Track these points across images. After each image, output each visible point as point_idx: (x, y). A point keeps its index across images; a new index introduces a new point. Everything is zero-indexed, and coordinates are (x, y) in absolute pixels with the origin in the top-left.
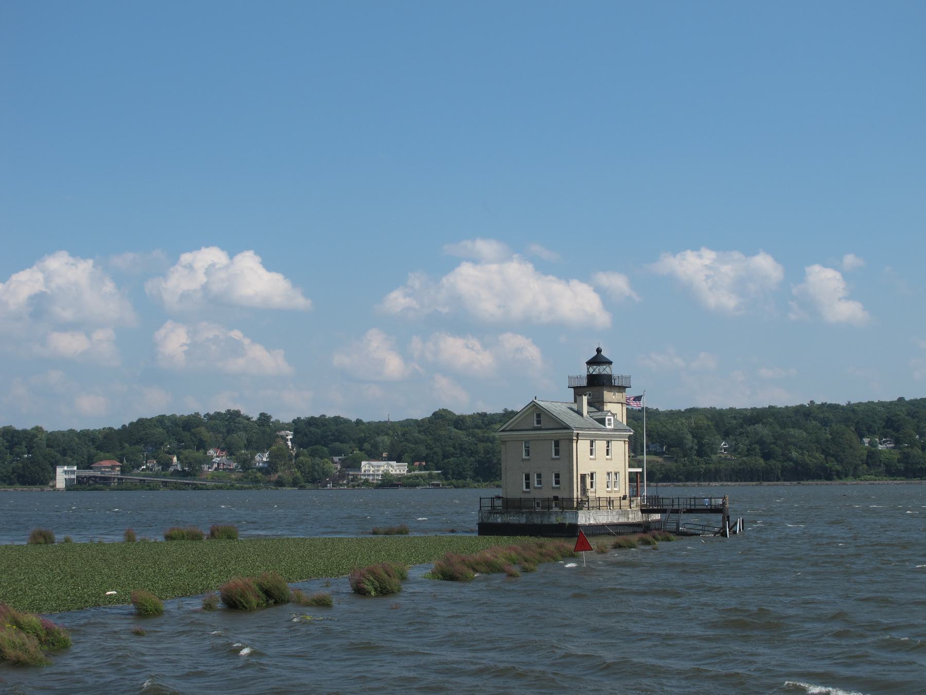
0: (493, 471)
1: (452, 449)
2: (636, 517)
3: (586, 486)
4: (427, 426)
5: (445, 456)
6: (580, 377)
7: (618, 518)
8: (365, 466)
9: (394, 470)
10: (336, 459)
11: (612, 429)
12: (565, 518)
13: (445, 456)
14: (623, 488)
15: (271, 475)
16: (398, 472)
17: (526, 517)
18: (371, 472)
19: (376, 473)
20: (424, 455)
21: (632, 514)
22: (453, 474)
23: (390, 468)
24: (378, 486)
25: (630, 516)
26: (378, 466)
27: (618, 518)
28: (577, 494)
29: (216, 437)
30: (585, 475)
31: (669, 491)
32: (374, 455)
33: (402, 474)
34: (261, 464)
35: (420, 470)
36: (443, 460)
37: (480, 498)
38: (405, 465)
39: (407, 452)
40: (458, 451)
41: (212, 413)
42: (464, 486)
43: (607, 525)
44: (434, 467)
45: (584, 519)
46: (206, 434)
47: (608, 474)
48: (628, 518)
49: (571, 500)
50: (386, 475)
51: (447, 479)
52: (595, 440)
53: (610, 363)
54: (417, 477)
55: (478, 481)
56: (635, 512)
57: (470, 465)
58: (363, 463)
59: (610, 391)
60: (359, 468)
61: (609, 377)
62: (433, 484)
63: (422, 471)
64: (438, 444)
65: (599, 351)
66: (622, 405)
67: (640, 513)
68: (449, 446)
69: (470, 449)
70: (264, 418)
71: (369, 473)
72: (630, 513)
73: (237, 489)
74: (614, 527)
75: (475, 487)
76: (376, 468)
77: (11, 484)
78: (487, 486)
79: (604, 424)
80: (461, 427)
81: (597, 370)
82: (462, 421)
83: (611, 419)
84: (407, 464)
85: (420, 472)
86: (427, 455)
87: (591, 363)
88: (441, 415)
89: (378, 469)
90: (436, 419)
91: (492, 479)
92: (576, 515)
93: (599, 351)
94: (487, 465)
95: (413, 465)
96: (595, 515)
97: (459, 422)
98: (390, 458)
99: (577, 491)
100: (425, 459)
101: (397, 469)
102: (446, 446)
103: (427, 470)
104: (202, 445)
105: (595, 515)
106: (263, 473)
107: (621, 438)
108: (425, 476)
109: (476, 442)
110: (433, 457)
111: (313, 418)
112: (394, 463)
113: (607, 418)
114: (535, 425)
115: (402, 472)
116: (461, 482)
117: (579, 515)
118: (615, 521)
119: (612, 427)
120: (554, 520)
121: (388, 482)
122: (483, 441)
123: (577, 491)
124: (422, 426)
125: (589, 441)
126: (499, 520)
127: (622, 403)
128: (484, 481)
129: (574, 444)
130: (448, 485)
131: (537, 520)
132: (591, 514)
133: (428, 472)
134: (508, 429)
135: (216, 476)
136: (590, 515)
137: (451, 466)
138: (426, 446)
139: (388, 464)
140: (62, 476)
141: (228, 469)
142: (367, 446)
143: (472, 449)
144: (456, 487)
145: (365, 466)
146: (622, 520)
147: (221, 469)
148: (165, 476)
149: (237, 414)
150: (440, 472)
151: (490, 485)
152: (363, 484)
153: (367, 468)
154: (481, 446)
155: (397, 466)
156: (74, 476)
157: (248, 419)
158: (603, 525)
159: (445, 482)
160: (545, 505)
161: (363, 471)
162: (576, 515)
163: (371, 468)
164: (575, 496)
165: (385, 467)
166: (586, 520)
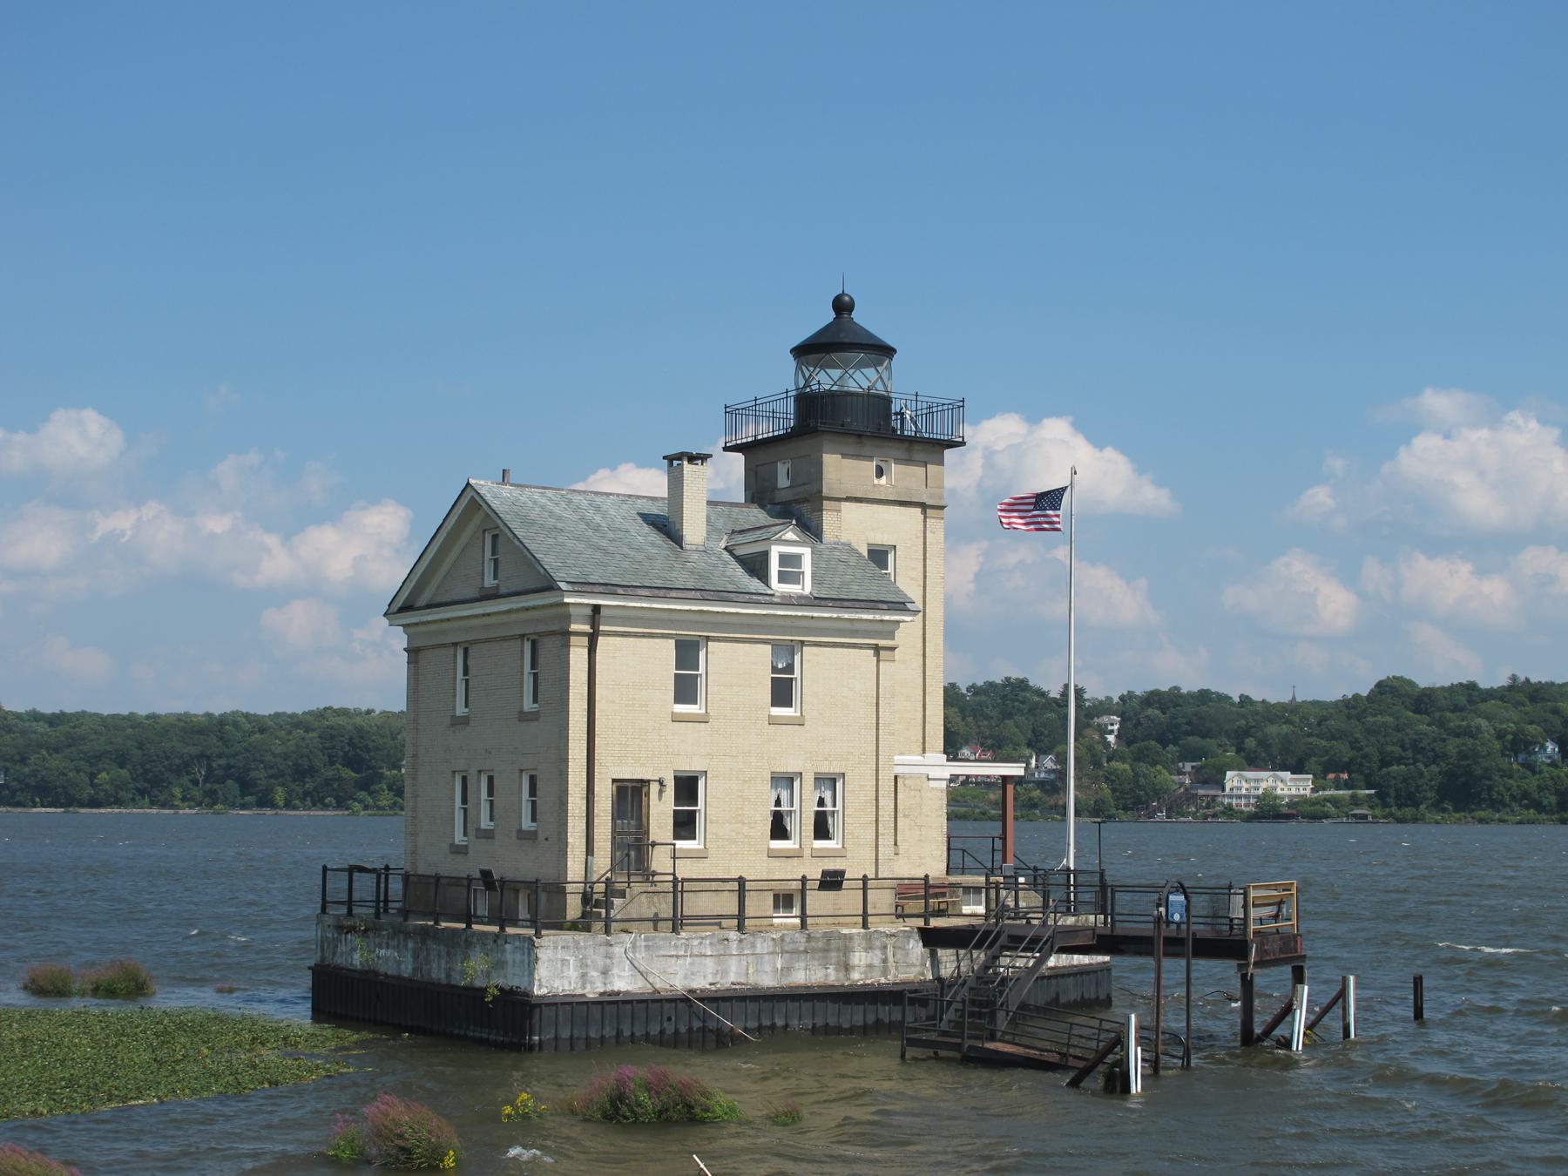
0: (1473, 791)
1: (1397, 750)
3: (647, 832)
4: (1363, 707)
6: (754, 409)
7: (787, 970)
8: (1232, 779)
9: (1286, 789)
11: (801, 597)
12: (500, 965)
13: (1385, 763)
15: (1059, 794)
16: (1294, 791)
17: (414, 950)
18: (1244, 792)
19: (1253, 792)
20: (1346, 759)
21: (869, 948)
22: (1398, 797)
23: (1279, 783)
24: (1251, 818)
25: (859, 958)
26: (1257, 780)
27: (787, 970)
29: (979, 727)
30: (645, 783)
32: (1253, 762)
33: (1302, 796)
34: (1043, 775)
35: (1338, 788)
36: (1380, 769)
37: (325, 869)
38: (1309, 779)
39: (1315, 755)
40: (1410, 754)
41: (980, 683)
42: (1415, 820)
43: (701, 1000)
44: (1362, 783)
45: (573, 973)
47: (785, 780)
48: (847, 968)
49: (558, 889)
51: (1385, 805)
52: (708, 639)
53: (885, 351)
55: (1444, 810)
56: (890, 942)
57: (1431, 780)
58: (1229, 774)
59: (858, 457)
61: (880, 405)
62: (1355, 816)
63: (1341, 789)
64: (1373, 739)
65: (842, 306)
66: (924, 513)
67: (916, 948)
68: (1394, 744)
69: (1433, 750)
71: (1239, 793)
72: (857, 943)
74: (752, 1007)
75: (1437, 822)
76: (1252, 784)
78: (1460, 819)
79: (763, 576)
80: (1426, 708)
81: (825, 379)
82: (1430, 697)
83: (785, 559)
84: (1311, 776)
85: (1336, 792)
86: (1352, 760)
87: (809, 351)
88: (1391, 687)
89: (1256, 785)
90: (1381, 694)
91: (1473, 807)
92: (529, 954)
93: (842, 306)
94: (1463, 779)
95: (1324, 778)
96: (640, 955)
97: (1424, 701)
99: (590, 850)
100: (1346, 767)
102: (1387, 744)
103: (1349, 789)
105: (640, 955)
106: (1046, 792)
107: (855, 634)
108: (1344, 800)
109: (1445, 736)
110: (1361, 765)
112: (1287, 775)
113: (775, 552)
114: (489, 581)
115: (1302, 792)
117: (541, 954)
118: (767, 979)
119: (806, 587)
121: (1268, 811)
122: (1457, 735)
123: (590, 850)
124: (1354, 707)
125: (672, 643)
126: (357, 960)
127: (923, 506)
128: (1456, 810)
129: (578, 656)
130: (1385, 817)
132: (618, 950)
133: (1350, 792)
134: (422, 602)
135: (961, 795)
136: (609, 956)
137: (1393, 782)
138: (1350, 742)
139: (1275, 776)
141: (984, 783)
142: (1250, 743)
143: (1437, 749)
144: (1400, 821)
145: (1232, 779)
146: (808, 974)
147: (971, 782)
149: (1022, 685)
150: (1373, 792)
151: (1466, 817)
152: (1223, 813)
153: (1235, 784)
155: (1291, 780)
157: (1042, 694)
158: (685, 1002)
159: (1378, 812)
161: (1227, 789)
162: (529, 954)
163: (1242, 784)
164: (575, 869)
165: (1271, 783)
166: (583, 975)
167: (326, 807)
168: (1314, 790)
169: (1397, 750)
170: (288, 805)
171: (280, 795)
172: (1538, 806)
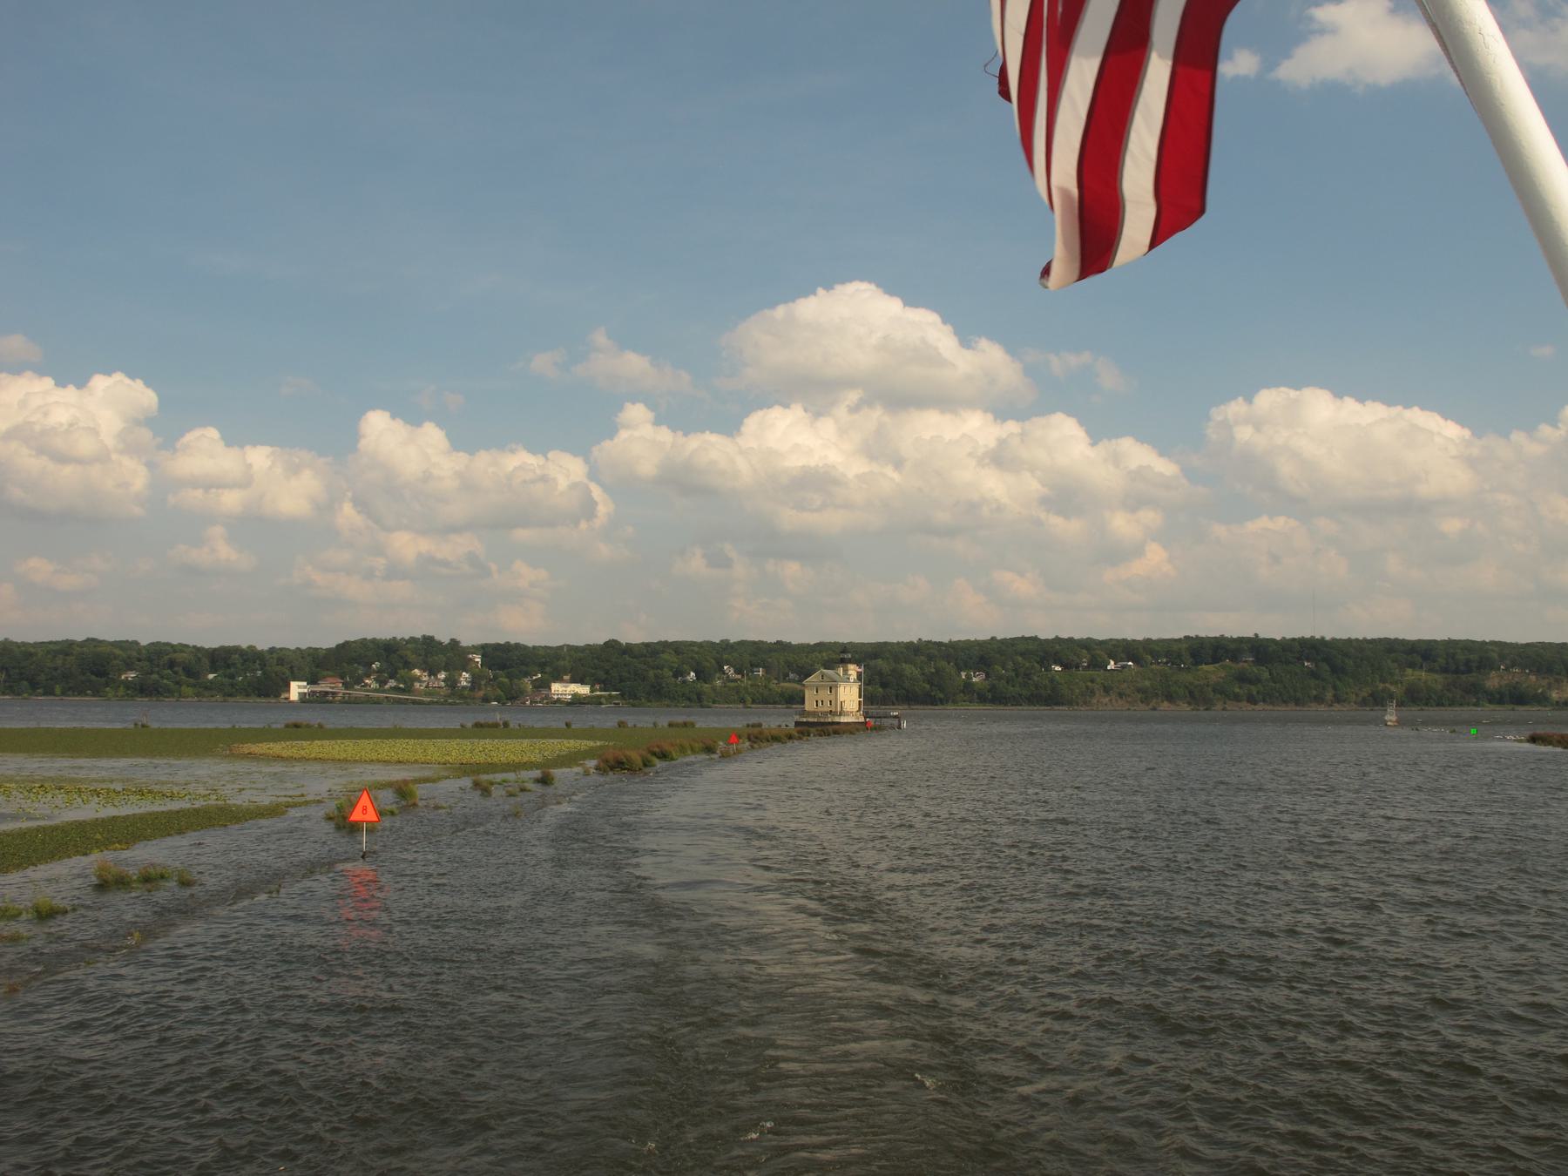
1: (627, 675)
2: (862, 719)
5: (622, 681)
10: (526, 680)
13: (622, 681)
14: (856, 707)
28: (839, 709)
31: (874, 709)
32: (559, 679)
46: (412, 658)
50: (575, 695)
54: (600, 696)
55: (650, 701)
60: (550, 689)
70: (454, 643)
73: (450, 704)
77: (248, 695)
97: (629, 650)
98: (573, 681)
101: (584, 690)
104: (409, 665)
111: (499, 645)
116: (636, 702)
120: (830, 720)
121: (577, 701)
122: (653, 668)
131: (822, 720)
140: (296, 689)
144: (633, 706)
148: (384, 692)
154: (651, 673)
156: (306, 691)
160: (825, 714)
163: (562, 690)
167: (87, 695)
168: (592, 691)
169: (627, 675)
170: (63, 694)
171: (58, 689)
172: (689, 699)
